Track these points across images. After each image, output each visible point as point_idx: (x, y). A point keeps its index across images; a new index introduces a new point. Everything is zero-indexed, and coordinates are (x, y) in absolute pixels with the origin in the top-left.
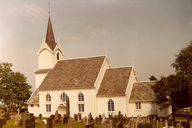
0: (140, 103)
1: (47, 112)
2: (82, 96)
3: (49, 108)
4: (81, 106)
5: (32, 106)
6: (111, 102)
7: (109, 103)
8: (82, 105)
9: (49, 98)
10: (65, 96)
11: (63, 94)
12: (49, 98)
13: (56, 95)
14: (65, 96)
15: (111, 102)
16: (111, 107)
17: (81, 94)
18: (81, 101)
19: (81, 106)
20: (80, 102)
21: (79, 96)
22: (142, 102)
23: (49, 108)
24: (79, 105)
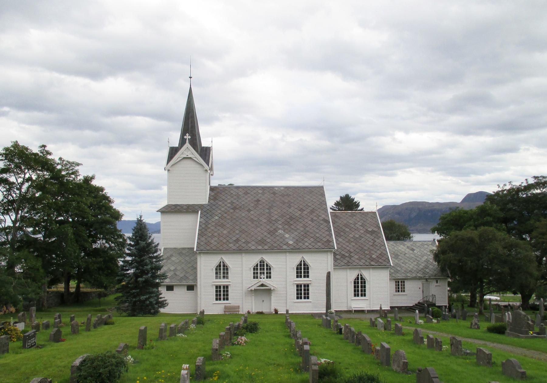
0: (404, 282)
1: (398, 293)
2: (304, 269)
3: (222, 293)
4: (303, 288)
5: (170, 288)
6: (360, 281)
7: (356, 282)
8: (401, 282)
9: (222, 270)
10: (265, 267)
11: (260, 262)
12: (222, 270)
13: (241, 267)
14: (265, 267)
15: (360, 281)
16: (360, 289)
17: (222, 264)
18: (303, 279)
19: (303, 288)
20: (299, 279)
21: (254, 269)
22: (176, 285)
23: (222, 293)
24: (218, 287)
